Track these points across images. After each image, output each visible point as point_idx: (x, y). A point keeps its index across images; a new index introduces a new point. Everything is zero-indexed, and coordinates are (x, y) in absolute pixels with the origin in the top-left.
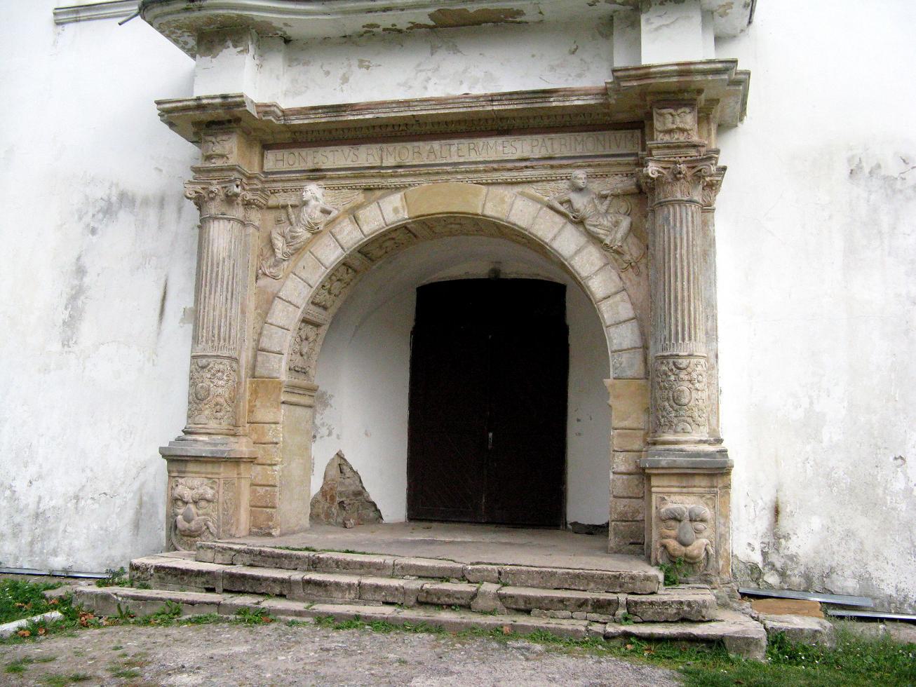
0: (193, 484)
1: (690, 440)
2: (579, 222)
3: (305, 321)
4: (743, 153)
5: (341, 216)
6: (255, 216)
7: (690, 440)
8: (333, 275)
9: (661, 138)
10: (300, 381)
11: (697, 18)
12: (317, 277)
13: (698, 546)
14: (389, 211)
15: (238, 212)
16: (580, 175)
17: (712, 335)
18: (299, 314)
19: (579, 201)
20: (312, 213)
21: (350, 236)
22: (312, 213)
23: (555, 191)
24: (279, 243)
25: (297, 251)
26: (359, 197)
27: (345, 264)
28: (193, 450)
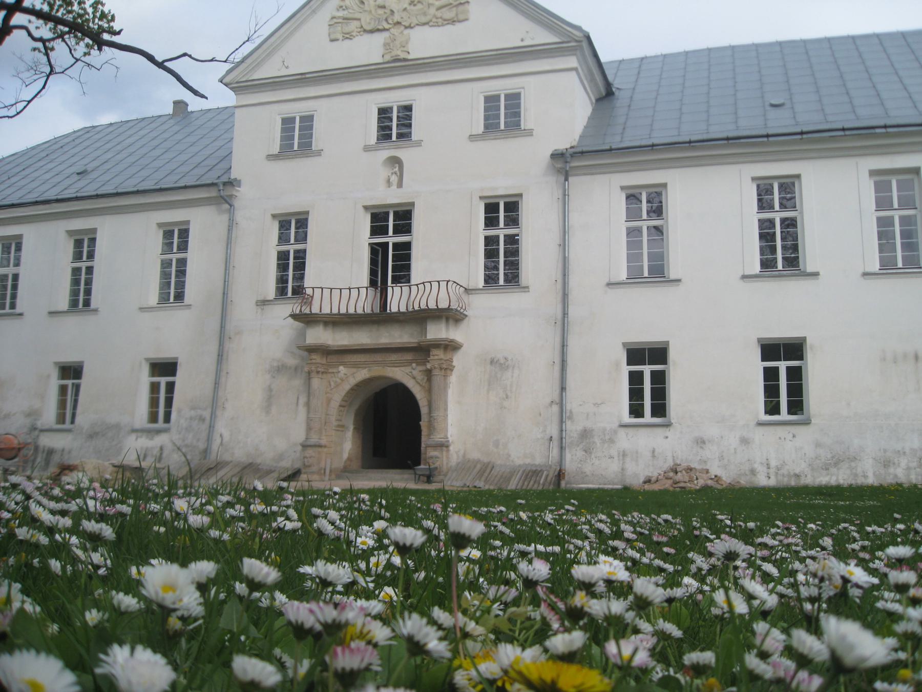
0: (310, 452)
1: (437, 438)
2: (414, 378)
3: (340, 406)
4: (458, 360)
5: (350, 376)
6: (325, 376)
7: (437, 438)
8: (348, 392)
9: (432, 357)
10: (340, 423)
11: (444, 321)
12: (343, 393)
13: (437, 464)
14: (363, 374)
15: (320, 375)
16: (414, 365)
17: (446, 410)
18: (338, 404)
19: (414, 372)
20: (341, 375)
21: (353, 381)
22: (341, 375)
23: (408, 369)
24: (332, 384)
25: (337, 386)
26: (354, 370)
27: (352, 389)
28: (308, 443)
